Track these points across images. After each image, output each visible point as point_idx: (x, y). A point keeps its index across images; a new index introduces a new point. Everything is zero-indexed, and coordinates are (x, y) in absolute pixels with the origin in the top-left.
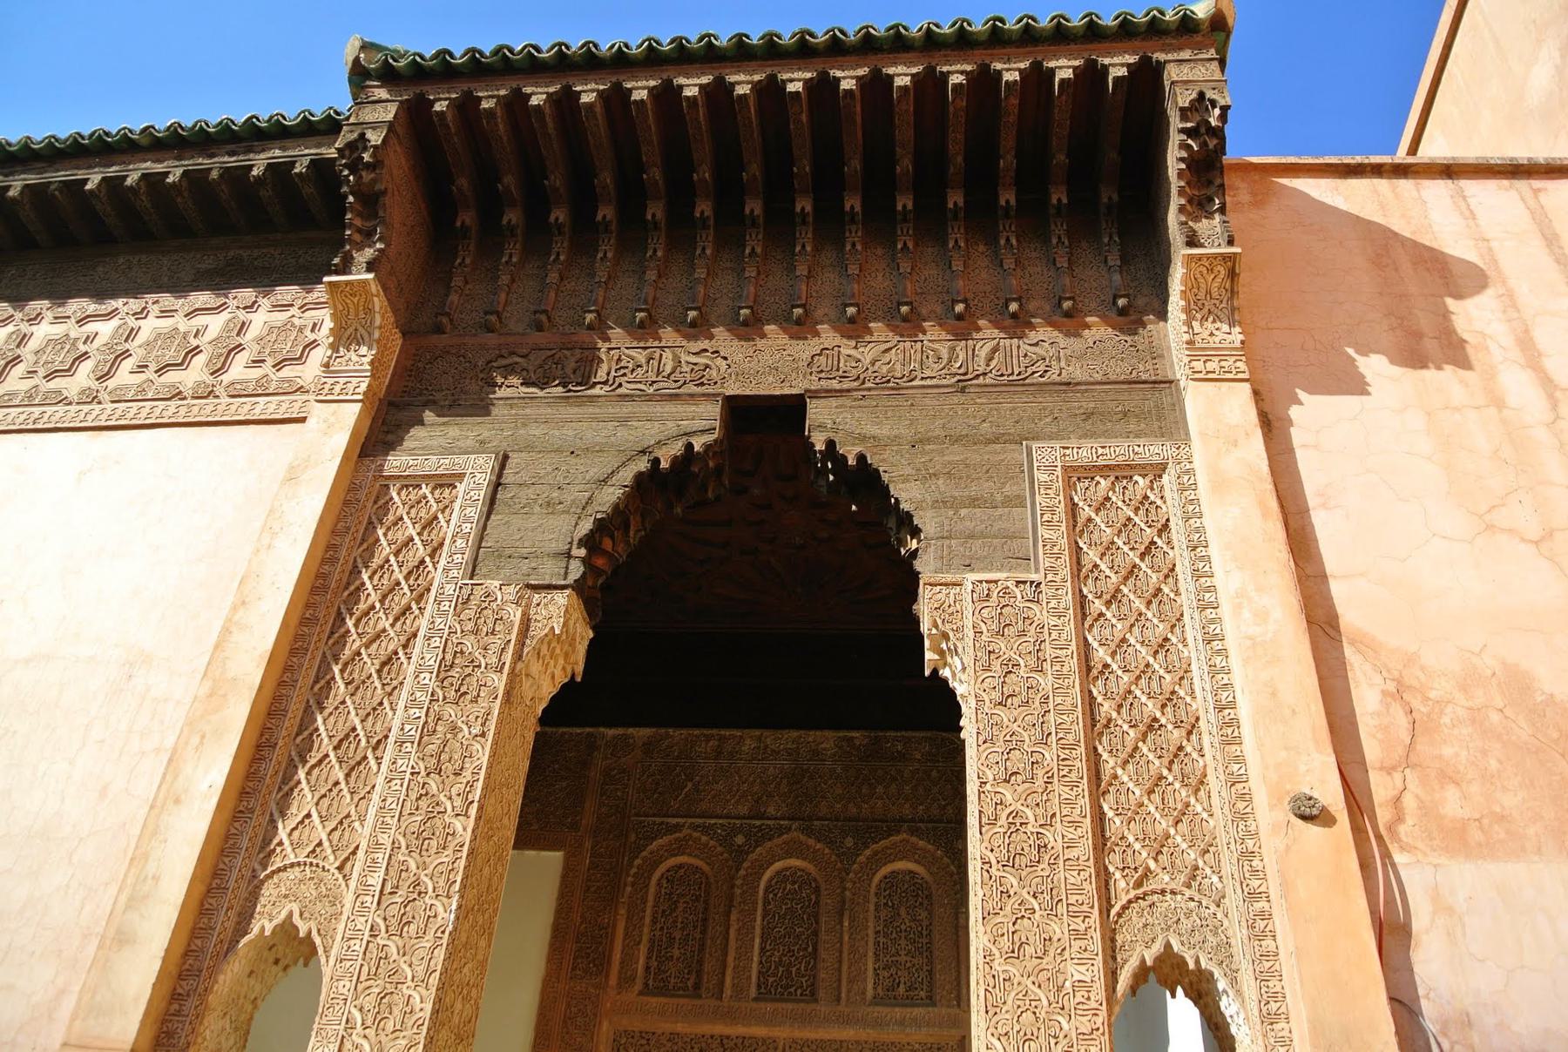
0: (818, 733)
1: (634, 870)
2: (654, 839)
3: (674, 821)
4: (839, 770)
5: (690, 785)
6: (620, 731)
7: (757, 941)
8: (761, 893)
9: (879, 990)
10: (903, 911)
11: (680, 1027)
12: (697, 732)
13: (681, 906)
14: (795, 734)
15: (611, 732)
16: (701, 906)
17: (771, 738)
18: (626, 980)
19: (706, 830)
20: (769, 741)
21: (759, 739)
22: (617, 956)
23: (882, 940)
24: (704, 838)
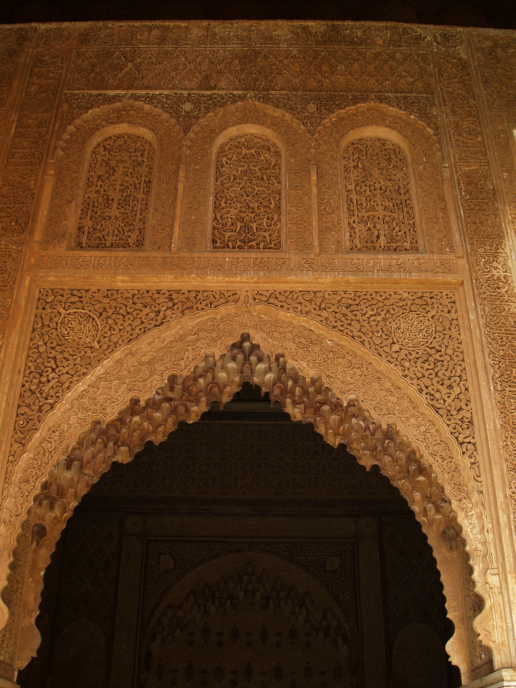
0: (271, 22)
1: (66, 136)
2: (88, 109)
3: (112, 93)
4: (295, 52)
5: (130, 65)
6: (54, 25)
7: (211, 199)
8: (214, 157)
9: (357, 241)
10: (376, 172)
11: (122, 281)
12: (138, 24)
13: (120, 170)
14: (246, 23)
15: (43, 27)
16: (144, 170)
17: (218, 27)
18: (53, 236)
19: (149, 99)
20: (217, 30)
21: (207, 29)
22: (43, 212)
23: (354, 197)
24: (147, 107)
